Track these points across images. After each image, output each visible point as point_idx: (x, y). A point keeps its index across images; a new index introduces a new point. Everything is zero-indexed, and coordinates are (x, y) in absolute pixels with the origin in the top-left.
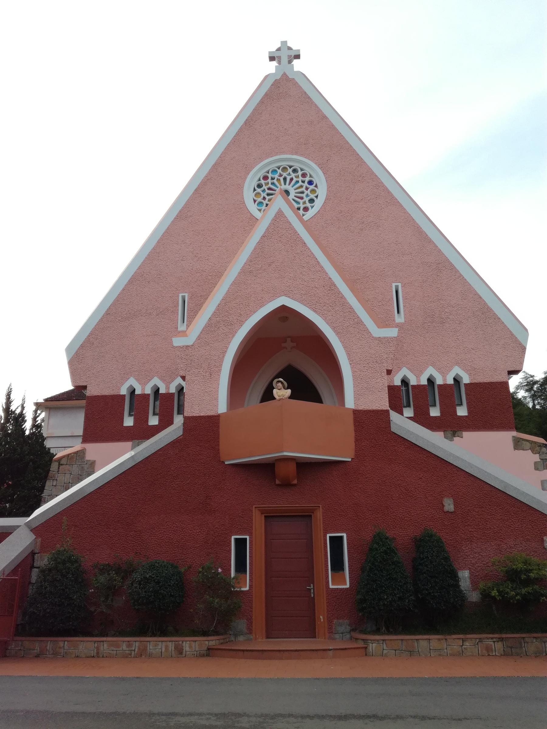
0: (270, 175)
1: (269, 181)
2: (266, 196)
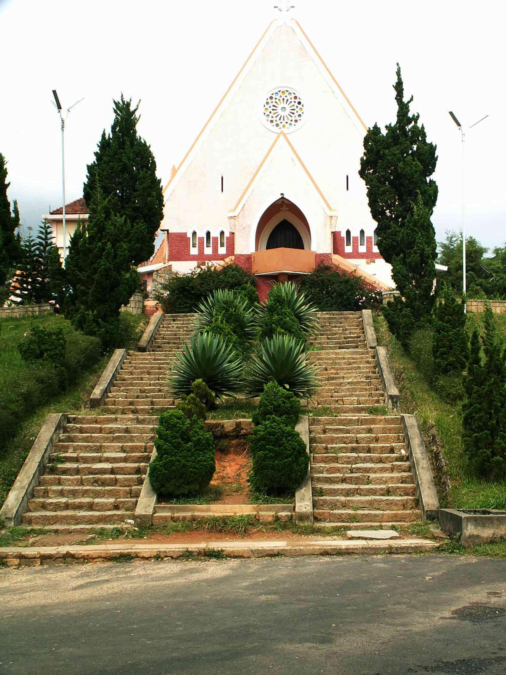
0: (274, 96)
1: (274, 100)
2: (272, 111)
